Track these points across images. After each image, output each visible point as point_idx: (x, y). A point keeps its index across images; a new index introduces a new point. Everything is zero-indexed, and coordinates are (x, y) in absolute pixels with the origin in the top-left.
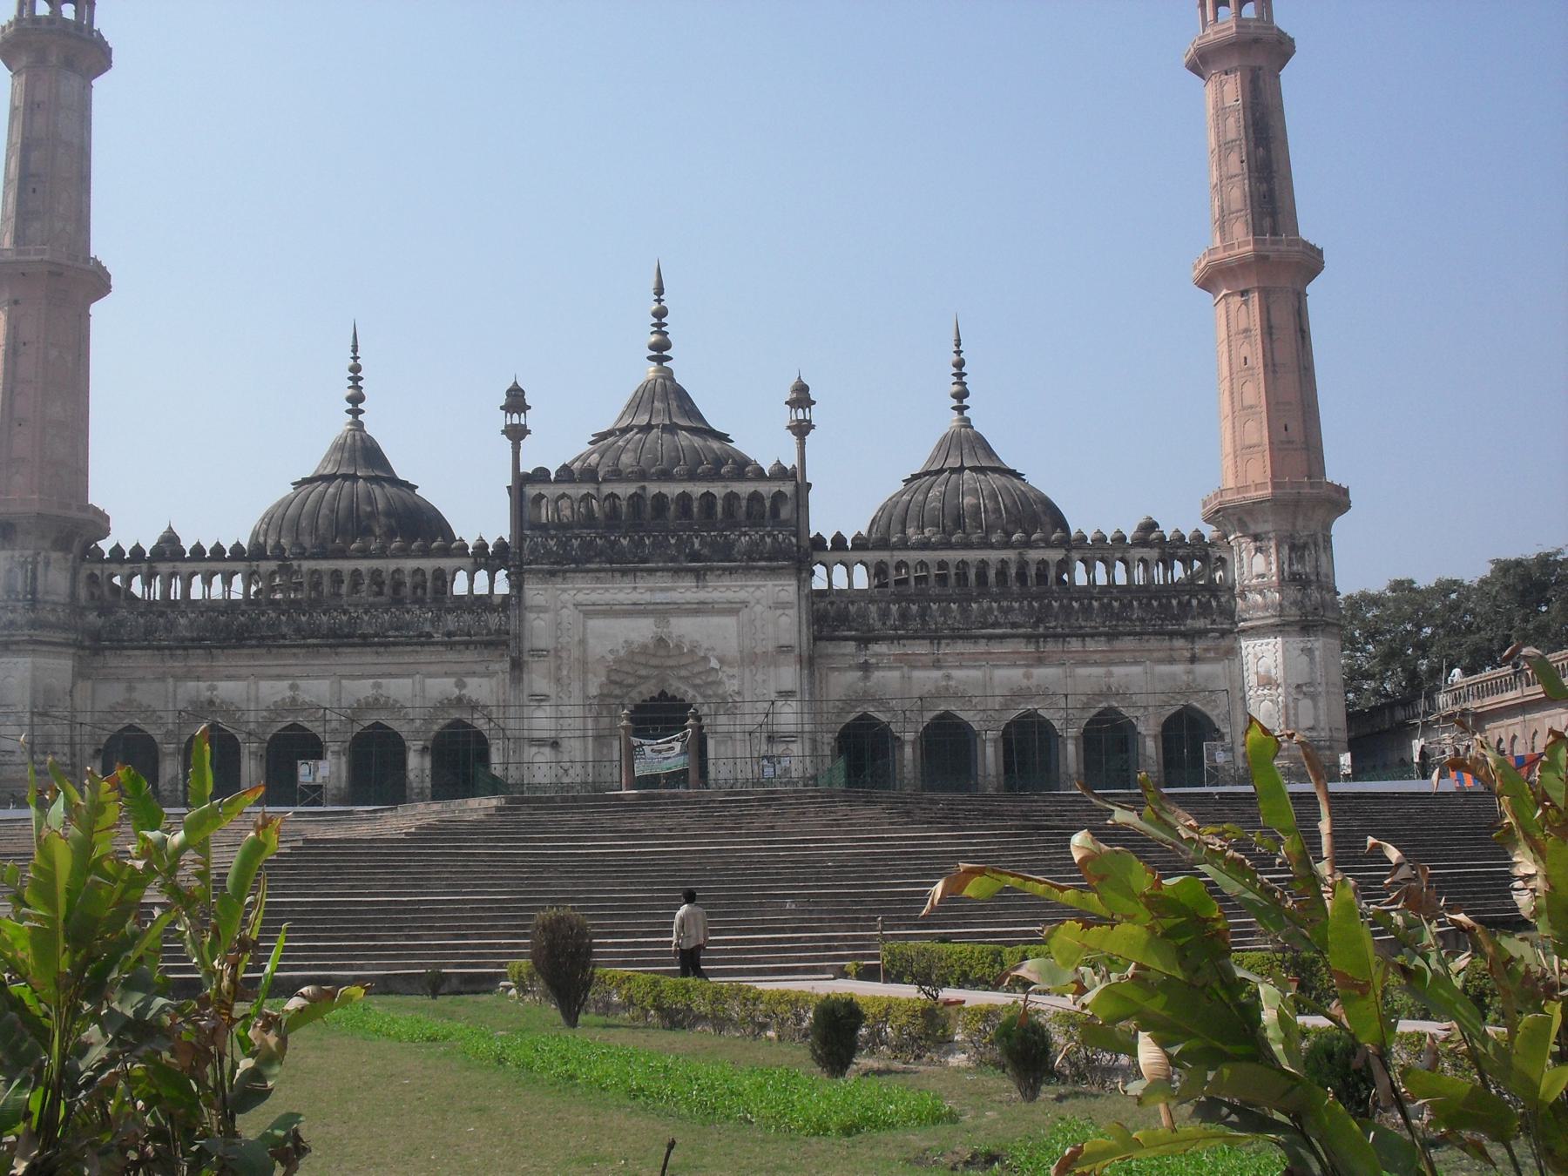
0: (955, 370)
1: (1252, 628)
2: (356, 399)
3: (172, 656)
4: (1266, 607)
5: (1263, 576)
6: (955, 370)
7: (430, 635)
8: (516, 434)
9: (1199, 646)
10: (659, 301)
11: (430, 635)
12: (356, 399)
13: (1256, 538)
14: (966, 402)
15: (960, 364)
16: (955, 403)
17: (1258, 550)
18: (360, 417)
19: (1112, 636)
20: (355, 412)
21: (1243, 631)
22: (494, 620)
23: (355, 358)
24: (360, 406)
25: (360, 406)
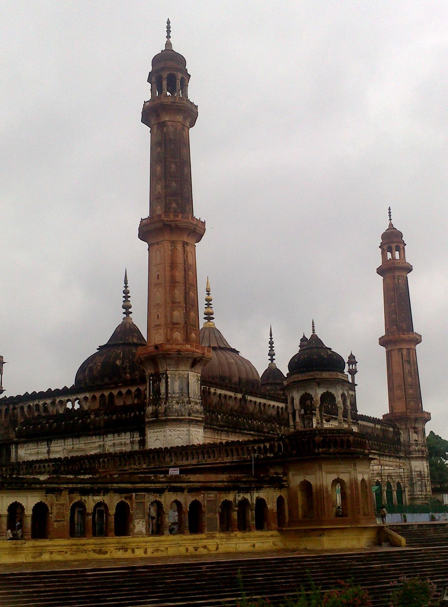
0: (270, 345)
1: (416, 457)
3: (217, 433)
4: (419, 451)
5: (417, 441)
6: (270, 345)
9: (401, 461)
10: (208, 294)
13: (414, 428)
14: (274, 357)
15: (271, 343)
16: (270, 357)
17: (416, 432)
19: (390, 456)
21: (413, 458)
24: (130, 310)
25: (130, 310)
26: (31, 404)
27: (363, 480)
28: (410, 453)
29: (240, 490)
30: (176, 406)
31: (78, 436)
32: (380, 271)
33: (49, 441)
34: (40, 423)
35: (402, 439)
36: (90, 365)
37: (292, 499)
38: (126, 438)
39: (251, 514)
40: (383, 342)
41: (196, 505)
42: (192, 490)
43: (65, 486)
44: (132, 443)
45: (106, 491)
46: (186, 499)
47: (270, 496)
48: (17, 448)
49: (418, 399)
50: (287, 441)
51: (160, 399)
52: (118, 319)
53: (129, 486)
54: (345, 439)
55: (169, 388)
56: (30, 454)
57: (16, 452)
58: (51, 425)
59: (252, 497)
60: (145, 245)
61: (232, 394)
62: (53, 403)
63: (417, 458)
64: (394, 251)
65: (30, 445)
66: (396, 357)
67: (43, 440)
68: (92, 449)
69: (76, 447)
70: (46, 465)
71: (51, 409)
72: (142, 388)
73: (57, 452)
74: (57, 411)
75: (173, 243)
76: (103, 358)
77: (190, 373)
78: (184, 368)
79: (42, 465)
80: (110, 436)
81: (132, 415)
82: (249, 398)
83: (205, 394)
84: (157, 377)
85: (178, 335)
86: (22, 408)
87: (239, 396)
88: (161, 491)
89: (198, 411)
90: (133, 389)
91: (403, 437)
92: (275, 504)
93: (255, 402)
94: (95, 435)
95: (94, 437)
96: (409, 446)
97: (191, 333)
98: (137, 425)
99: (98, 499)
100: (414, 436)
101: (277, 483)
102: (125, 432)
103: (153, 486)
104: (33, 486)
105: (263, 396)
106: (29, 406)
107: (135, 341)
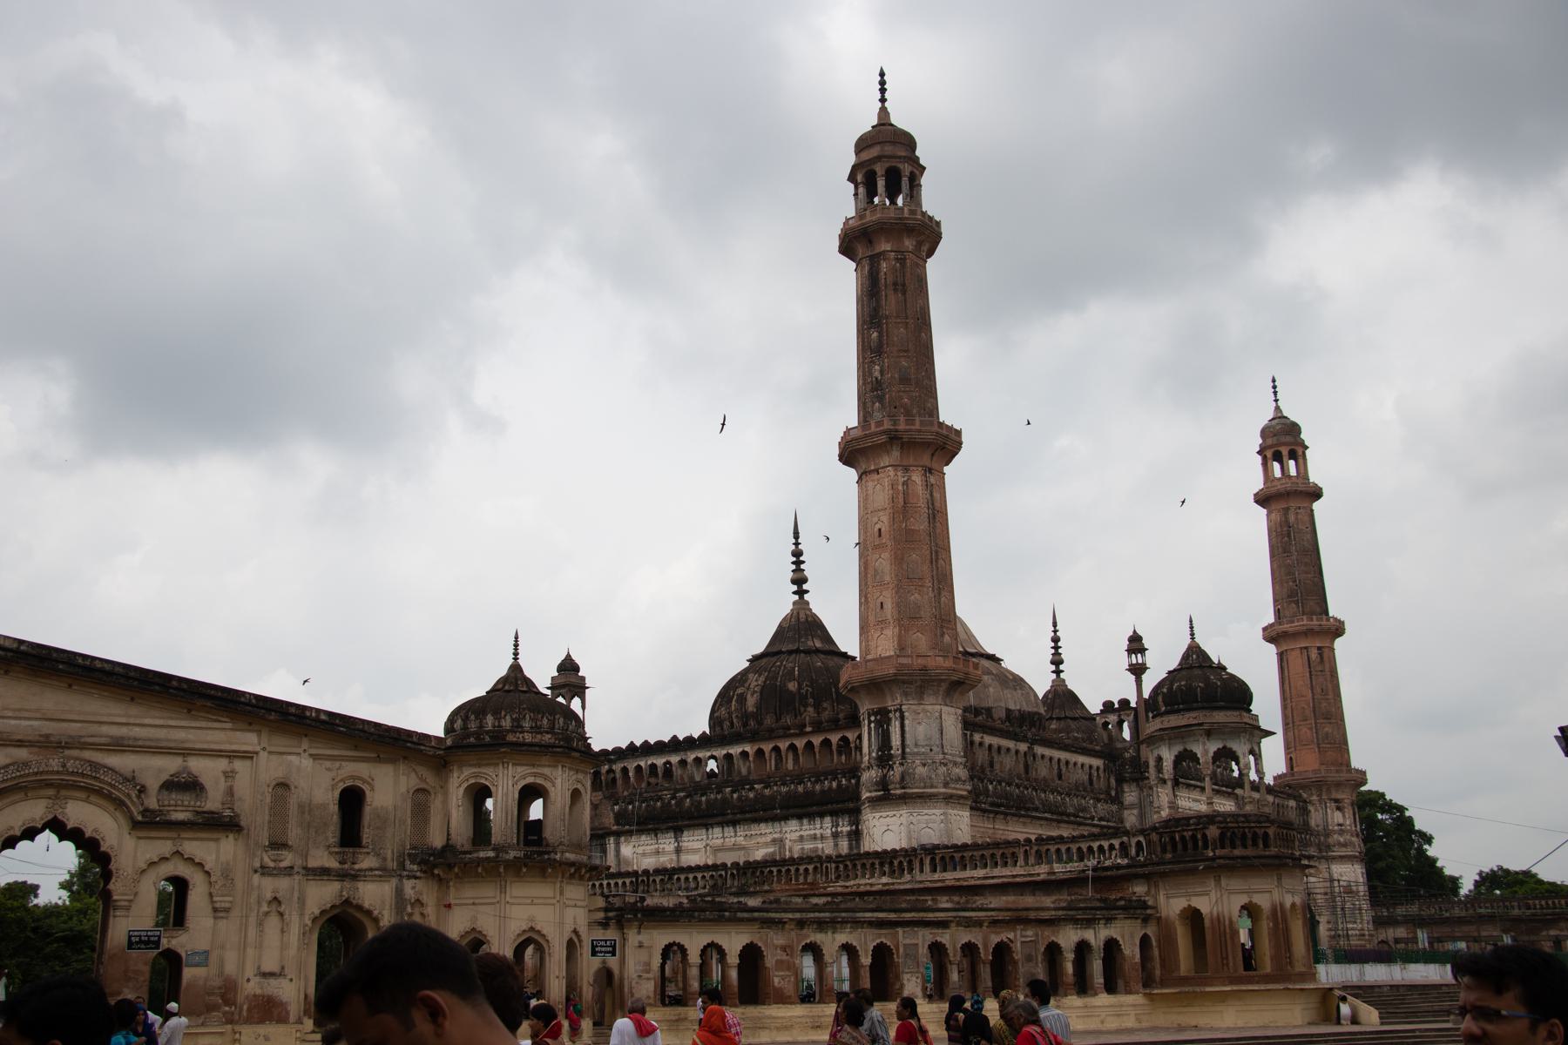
1: (1341, 857)
2: (799, 580)
4: (1345, 845)
7: (1092, 818)
8: (1138, 671)
11: (1092, 818)
12: (799, 580)
15: (1056, 640)
17: (1338, 808)
18: (806, 597)
20: (801, 593)
21: (1334, 858)
22: (1114, 808)
23: (797, 544)
24: (805, 587)
25: (805, 587)
26: (642, 764)
27: (1293, 905)
28: (1329, 848)
29: (1075, 921)
30: (921, 770)
31: (734, 823)
32: (1262, 499)
33: (678, 831)
34: (660, 798)
35: (1313, 823)
36: (739, 691)
37: (1168, 940)
38: (825, 826)
39: (1096, 967)
40: (1271, 635)
41: (1002, 950)
42: (994, 922)
43: (790, 916)
44: (835, 835)
45: (857, 924)
46: (986, 940)
47: (1127, 934)
48: (618, 844)
49: (1342, 745)
50: (1154, 837)
51: (891, 757)
52: (784, 603)
53: (892, 916)
54: (1260, 832)
55: (907, 736)
56: (644, 854)
57: (618, 851)
58: (680, 802)
59: (1096, 937)
60: (851, 474)
61: (1010, 744)
62: (683, 763)
63: (1342, 859)
64: (1285, 459)
65: (643, 837)
66: (1297, 663)
67: (668, 830)
68: (759, 846)
69: (730, 842)
70: (699, 876)
71: (677, 772)
72: (851, 736)
73: (696, 851)
74: (692, 778)
75: (906, 469)
76: (762, 679)
77: (945, 709)
78: (932, 699)
79: (691, 876)
80: (793, 825)
81: (834, 784)
82: (1039, 750)
83: (969, 746)
84: (882, 718)
85: (921, 641)
86: (625, 770)
87: (1023, 747)
88: (943, 924)
89: (959, 779)
90: (834, 738)
91: (1315, 819)
92: (1137, 950)
93: (1051, 759)
94: (765, 820)
95: (763, 825)
96: (1328, 834)
97: (942, 635)
98: (844, 805)
99: (842, 937)
100: (1338, 817)
101: (1140, 911)
102: (822, 815)
103: (930, 916)
104: (739, 915)
105: (1065, 748)
106: (639, 768)
107: (818, 644)
